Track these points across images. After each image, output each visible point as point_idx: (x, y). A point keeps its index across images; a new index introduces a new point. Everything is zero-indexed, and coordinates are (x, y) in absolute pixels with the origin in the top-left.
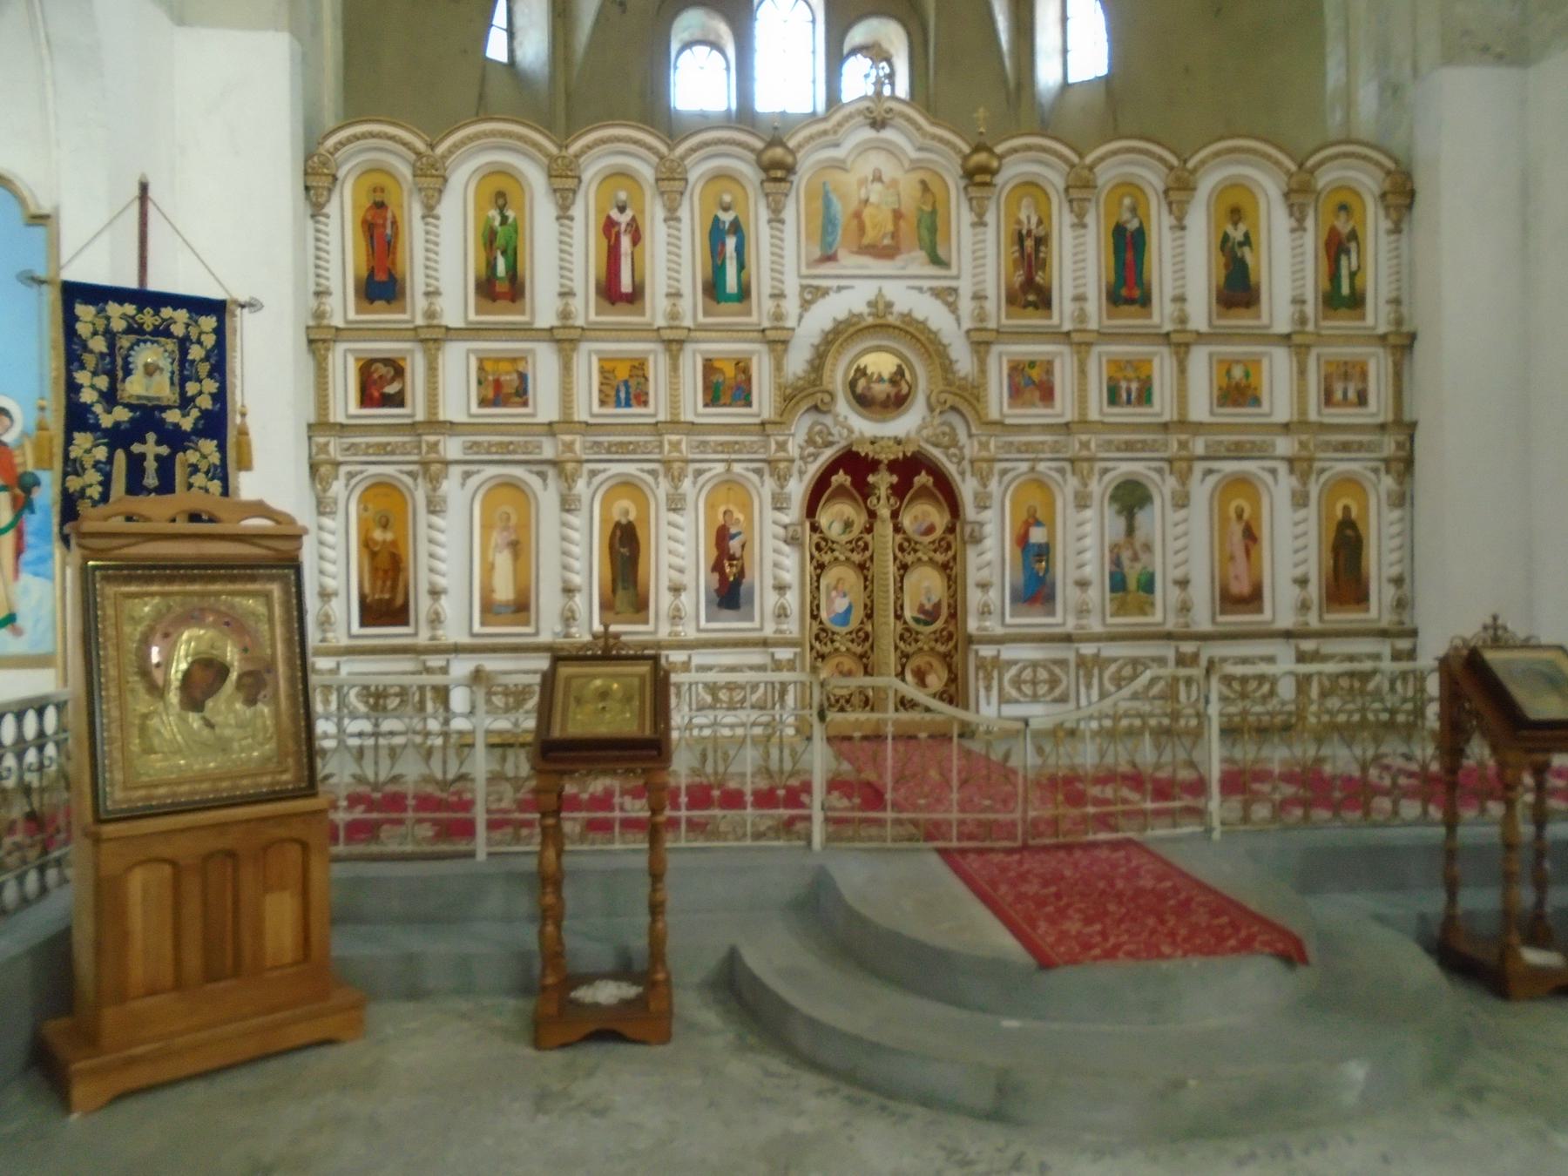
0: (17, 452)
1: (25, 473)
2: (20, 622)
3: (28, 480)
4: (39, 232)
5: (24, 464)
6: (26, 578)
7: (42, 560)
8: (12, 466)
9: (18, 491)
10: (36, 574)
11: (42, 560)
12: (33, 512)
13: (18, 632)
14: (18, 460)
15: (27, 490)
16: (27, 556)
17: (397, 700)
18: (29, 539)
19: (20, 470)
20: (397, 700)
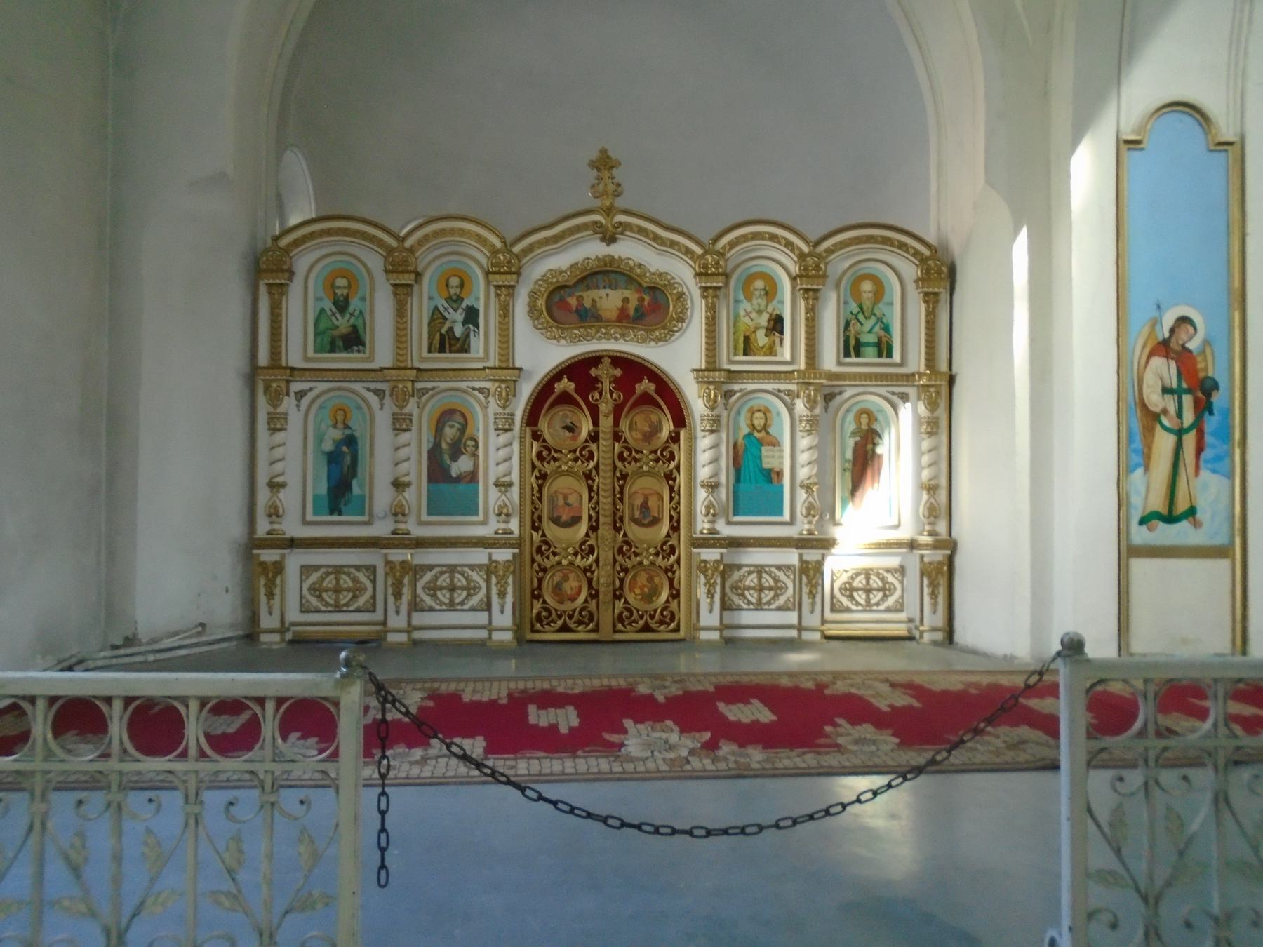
0: (1199, 359)
1: (1207, 378)
2: (1199, 515)
3: (1208, 384)
4: (1220, 158)
5: (1206, 369)
6: (1205, 474)
7: (1218, 458)
8: (1196, 371)
9: (1200, 395)
10: (1214, 471)
11: (1218, 458)
12: (1211, 413)
13: (1197, 525)
14: (1200, 366)
15: (1208, 394)
16: (1203, 456)
17: (880, 594)
18: (1209, 439)
19: (1202, 375)
20: (880, 594)
